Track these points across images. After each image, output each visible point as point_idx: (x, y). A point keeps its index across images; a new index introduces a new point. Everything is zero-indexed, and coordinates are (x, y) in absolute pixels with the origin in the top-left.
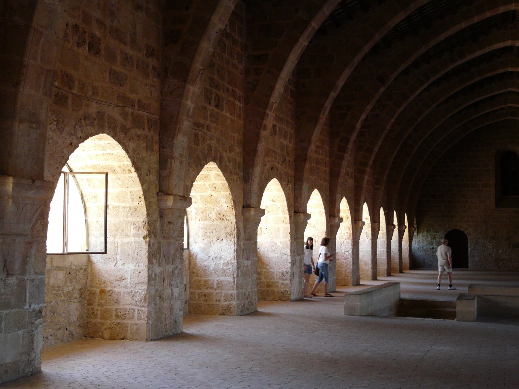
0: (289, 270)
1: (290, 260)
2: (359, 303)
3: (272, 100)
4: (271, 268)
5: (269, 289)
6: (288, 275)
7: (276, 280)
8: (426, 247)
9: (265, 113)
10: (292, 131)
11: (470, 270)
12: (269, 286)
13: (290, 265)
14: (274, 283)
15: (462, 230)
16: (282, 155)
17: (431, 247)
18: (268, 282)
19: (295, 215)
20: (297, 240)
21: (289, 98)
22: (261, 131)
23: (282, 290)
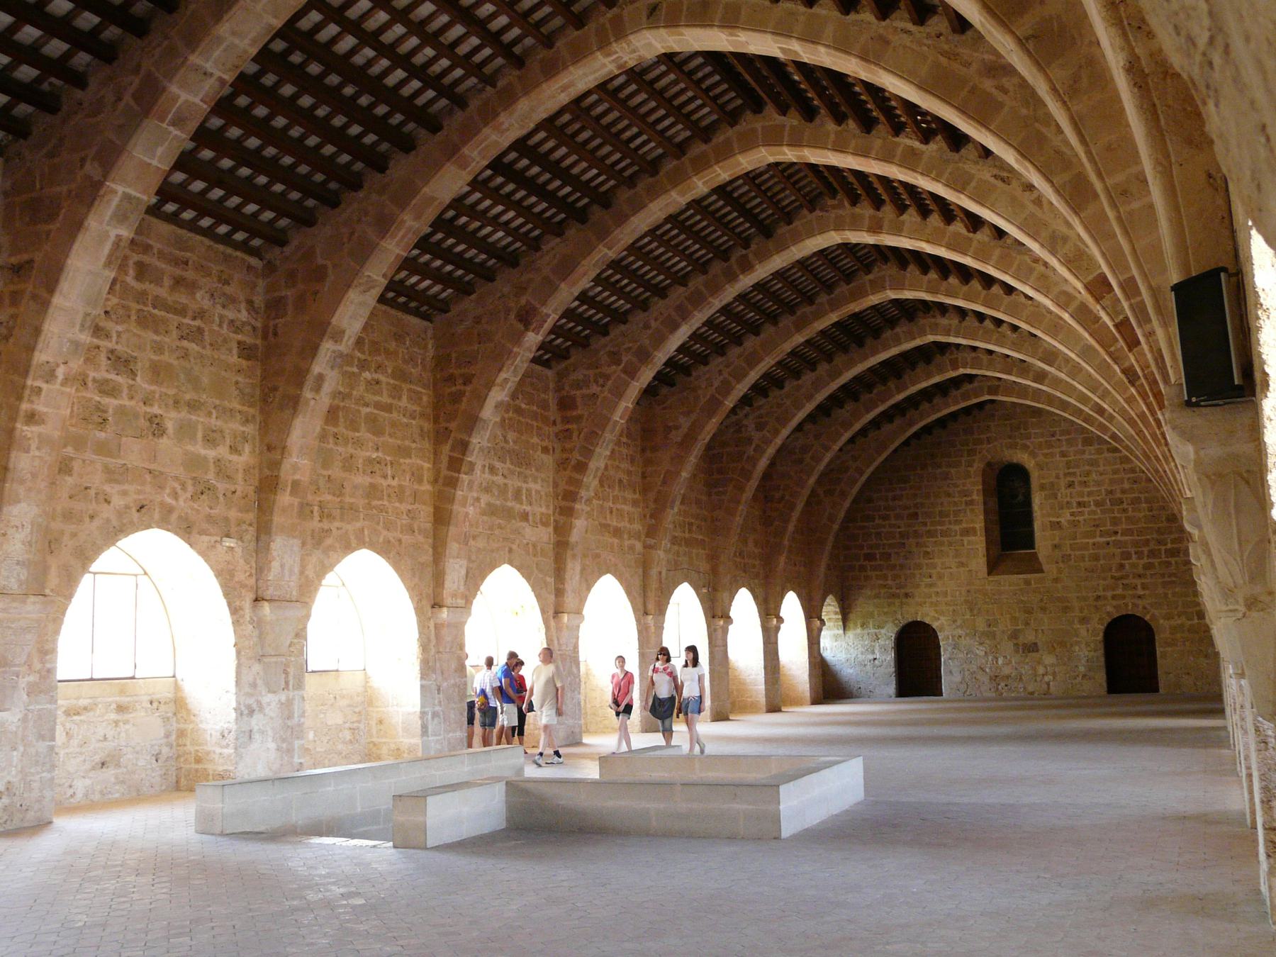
0: (233, 726)
1: (234, 705)
2: (221, 805)
3: (40, 357)
4: (201, 721)
5: (200, 766)
6: (232, 737)
7: (209, 748)
8: (861, 657)
9: (24, 387)
10: (250, 429)
11: (948, 701)
12: (198, 761)
13: (233, 715)
14: (208, 753)
15: (927, 620)
16: (194, 479)
17: (871, 657)
18: (197, 751)
19: (255, 607)
20: (266, 660)
21: (234, 359)
22: (18, 425)
23: (221, 768)
